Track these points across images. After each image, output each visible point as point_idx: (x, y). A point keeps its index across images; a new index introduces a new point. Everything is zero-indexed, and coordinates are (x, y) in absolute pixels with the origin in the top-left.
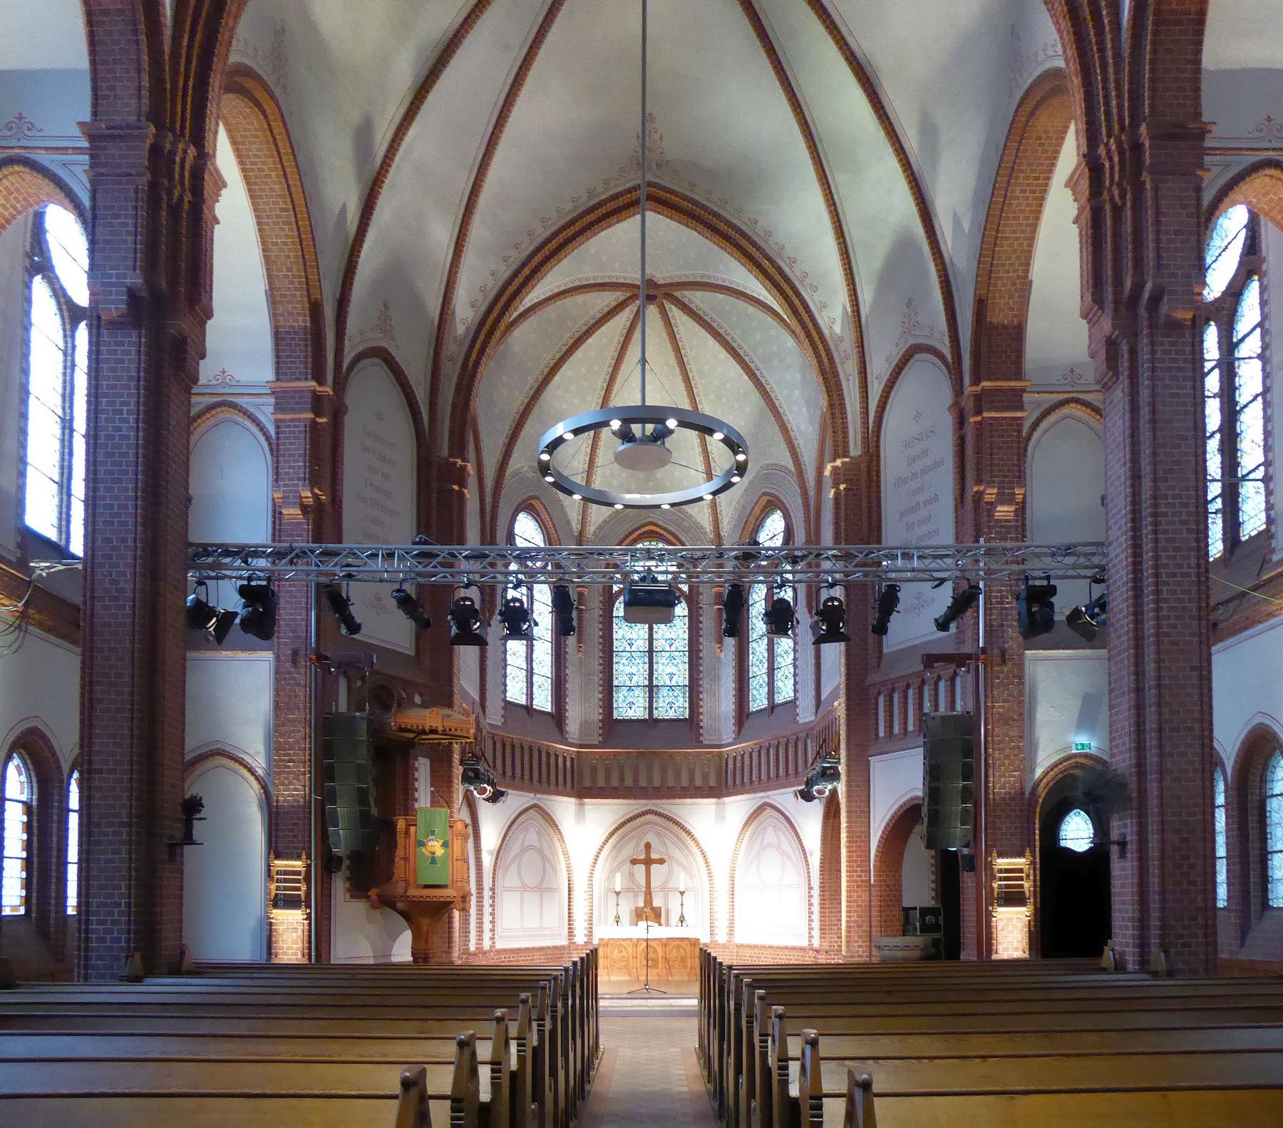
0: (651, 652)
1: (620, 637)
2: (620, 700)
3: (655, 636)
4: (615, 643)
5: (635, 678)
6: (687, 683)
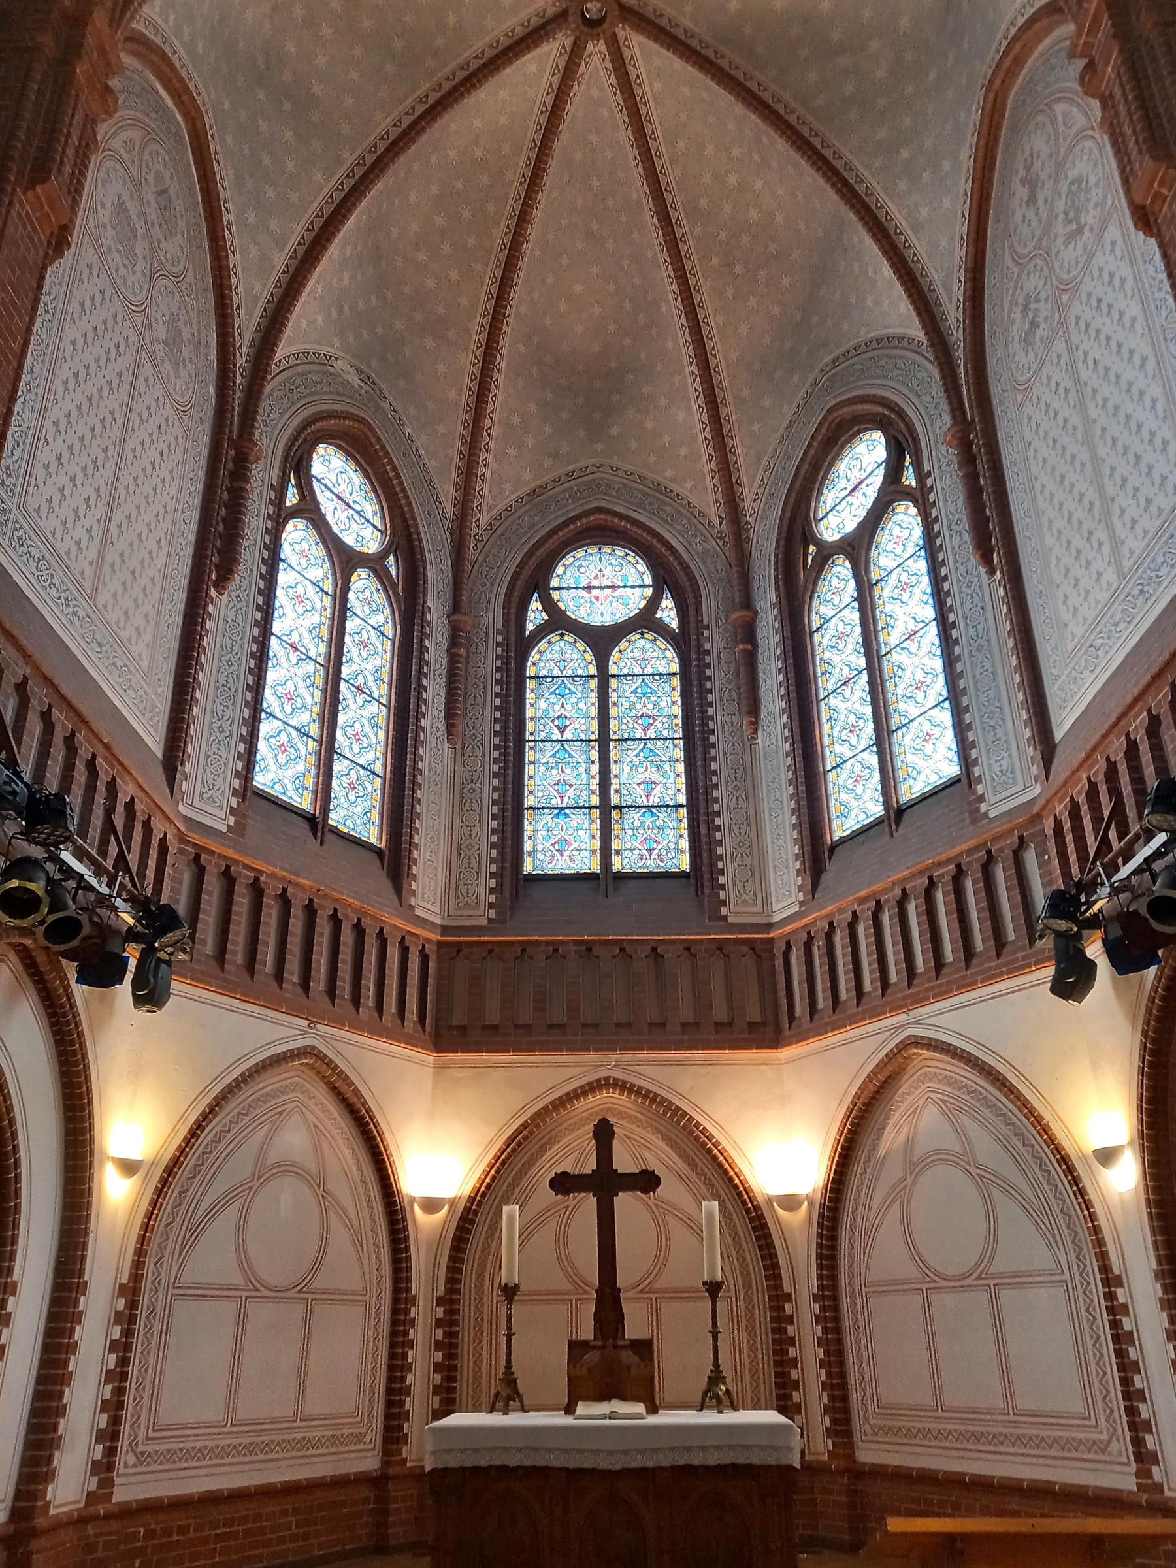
0: (604, 740)
1: (540, 713)
2: (539, 836)
3: (613, 712)
4: (530, 726)
5: (571, 792)
6: (682, 799)
